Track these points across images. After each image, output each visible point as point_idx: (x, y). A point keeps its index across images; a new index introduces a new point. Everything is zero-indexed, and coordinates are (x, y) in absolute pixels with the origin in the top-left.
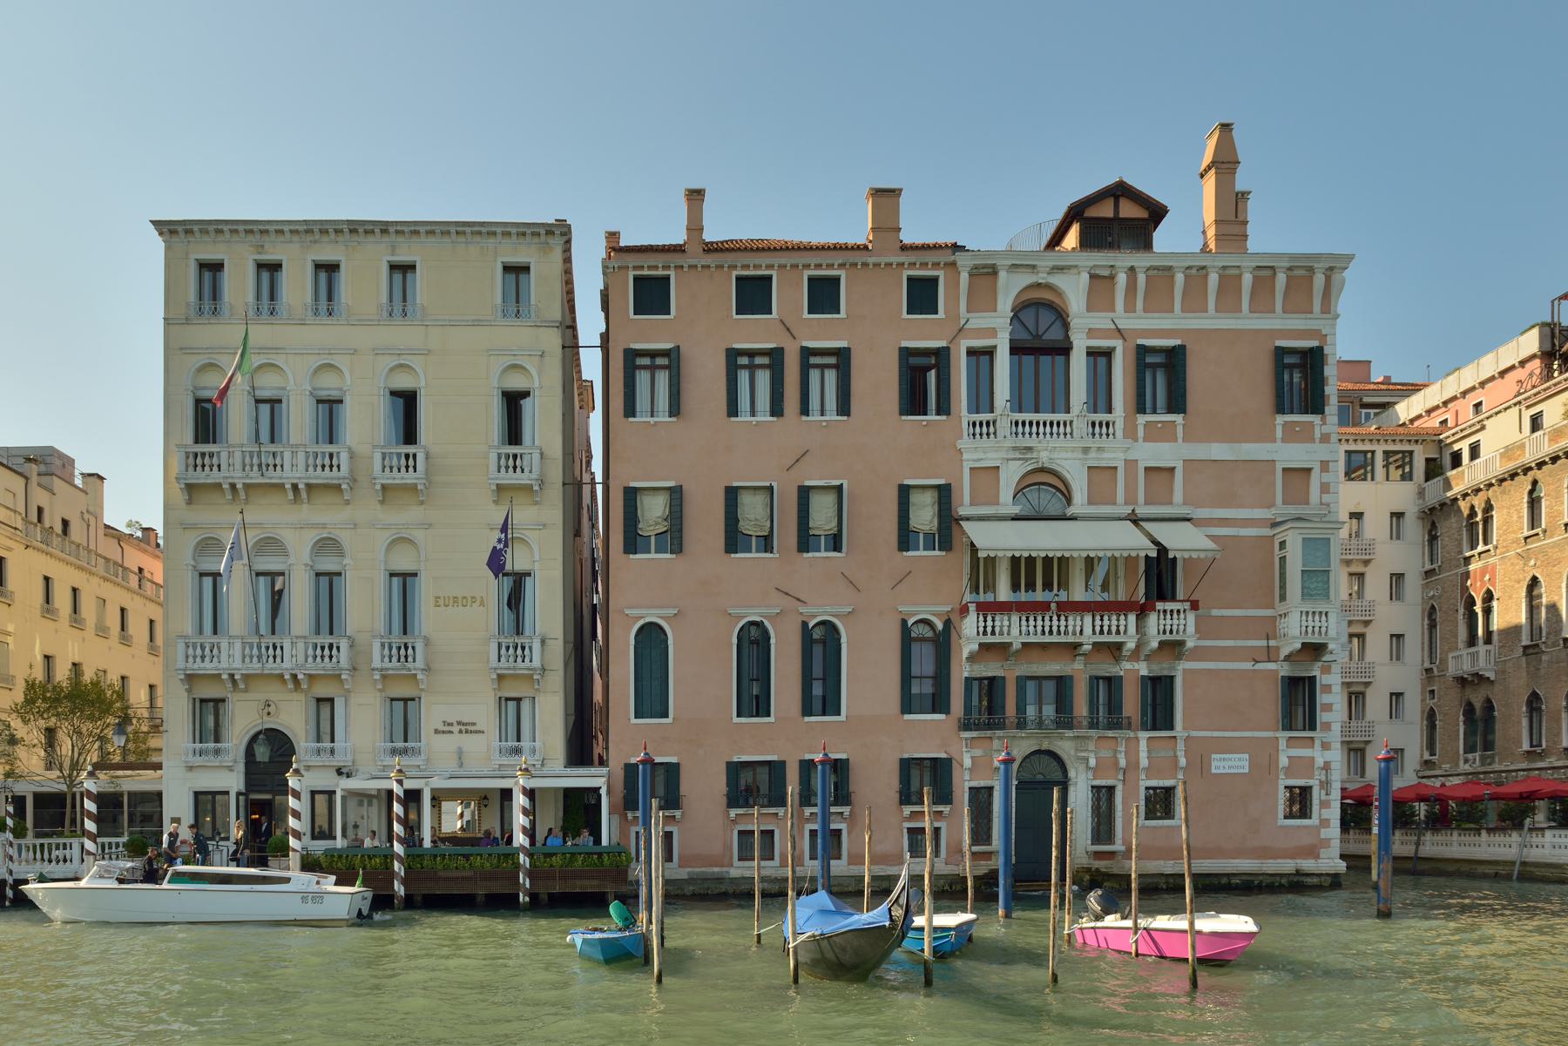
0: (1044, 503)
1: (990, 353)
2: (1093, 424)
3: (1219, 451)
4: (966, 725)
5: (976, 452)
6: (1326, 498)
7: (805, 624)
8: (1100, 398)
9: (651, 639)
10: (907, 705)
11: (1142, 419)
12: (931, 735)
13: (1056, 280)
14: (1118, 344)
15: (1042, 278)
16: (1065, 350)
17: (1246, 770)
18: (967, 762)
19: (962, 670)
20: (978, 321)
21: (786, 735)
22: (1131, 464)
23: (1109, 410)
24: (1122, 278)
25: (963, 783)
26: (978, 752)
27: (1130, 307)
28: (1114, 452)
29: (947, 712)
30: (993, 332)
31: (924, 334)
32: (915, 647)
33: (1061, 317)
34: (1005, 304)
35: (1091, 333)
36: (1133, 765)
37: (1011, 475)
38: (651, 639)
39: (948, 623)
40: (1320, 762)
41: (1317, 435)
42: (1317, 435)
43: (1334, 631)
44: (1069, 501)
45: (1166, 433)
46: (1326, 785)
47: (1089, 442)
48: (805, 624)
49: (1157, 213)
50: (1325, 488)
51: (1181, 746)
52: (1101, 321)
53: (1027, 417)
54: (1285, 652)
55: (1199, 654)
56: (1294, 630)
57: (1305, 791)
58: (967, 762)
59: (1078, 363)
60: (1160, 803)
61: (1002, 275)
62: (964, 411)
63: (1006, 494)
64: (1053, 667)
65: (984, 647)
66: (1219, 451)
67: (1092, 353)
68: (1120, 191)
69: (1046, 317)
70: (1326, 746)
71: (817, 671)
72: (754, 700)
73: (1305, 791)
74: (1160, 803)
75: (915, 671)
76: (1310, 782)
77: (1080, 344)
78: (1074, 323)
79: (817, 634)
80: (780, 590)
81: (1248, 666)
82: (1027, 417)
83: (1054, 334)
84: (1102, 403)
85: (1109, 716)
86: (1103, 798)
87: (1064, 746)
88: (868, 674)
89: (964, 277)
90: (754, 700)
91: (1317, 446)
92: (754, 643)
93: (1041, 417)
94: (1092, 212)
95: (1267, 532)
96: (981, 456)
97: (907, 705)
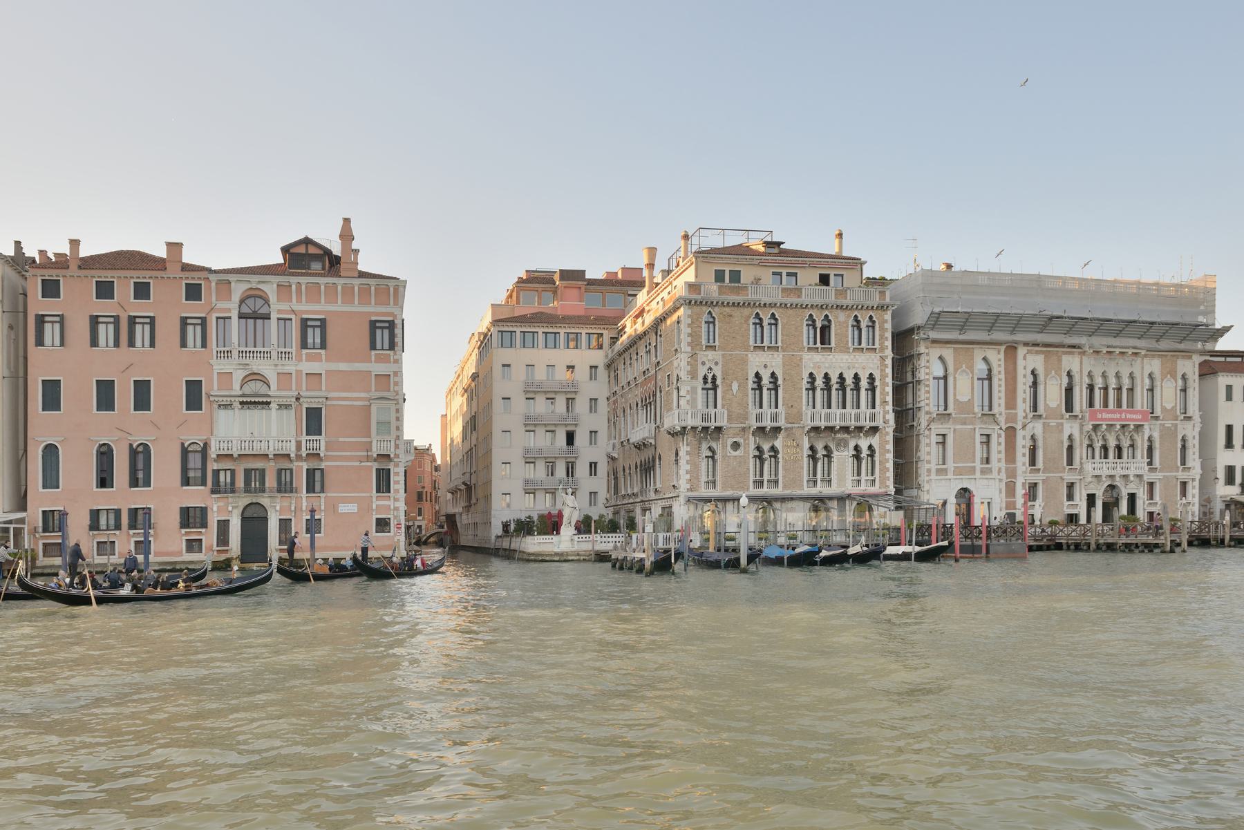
3: (343, 366)
4: (213, 492)
5: (220, 366)
7: (131, 445)
8: (284, 340)
9: (51, 452)
10: (186, 481)
11: (304, 351)
12: (196, 496)
14: (293, 317)
15: (254, 286)
16: (267, 317)
18: (215, 509)
19: (212, 466)
20: (221, 305)
21: (122, 496)
22: (299, 372)
25: (213, 519)
26: (221, 504)
27: (299, 300)
28: (290, 367)
30: (229, 310)
31: (194, 310)
32: (191, 456)
33: (267, 302)
34: (236, 297)
35: (279, 311)
36: (298, 510)
37: (238, 376)
38: (51, 452)
39: (205, 444)
45: (318, 358)
47: (276, 362)
48: (131, 445)
51: (323, 500)
52: (284, 306)
55: (328, 458)
58: (215, 509)
60: (313, 526)
63: (236, 386)
64: (259, 465)
65: (218, 456)
66: (343, 366)
69: (260, 302)
71: (140, 465)
72: (104, 481)
74: (313, 526)
75: (191, 465)
77: (274, 316)
79: (140, 449)
80: (123, 427)
81: (357, 464)
83: (264, 311)
85: (285, 487)
86: (285, 524)
87: (264, 500)
88: (165, 467)
89: (213, 284)
90: (104, 481)
92: (105, 455)
95: (367, 403)
97: (186, 481)
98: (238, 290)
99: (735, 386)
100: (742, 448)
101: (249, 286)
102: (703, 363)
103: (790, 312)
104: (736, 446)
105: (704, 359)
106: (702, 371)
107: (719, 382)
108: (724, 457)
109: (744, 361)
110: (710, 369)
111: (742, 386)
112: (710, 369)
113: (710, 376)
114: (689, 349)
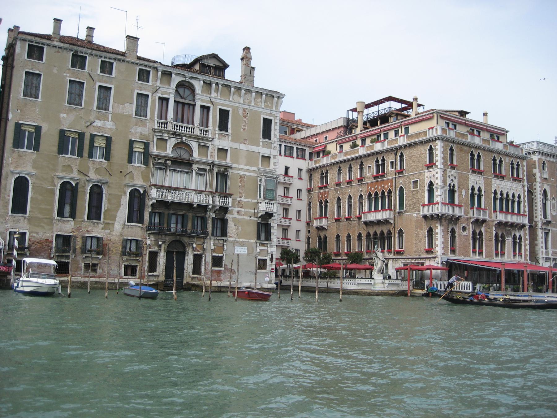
0: (182, 154)
1: (167, 100)
2: (201, 130)
6: (275, 167)
13: (192, 81)
15: (187, 80)
17: (246, 253)
23: (207, 127)
24: (214, 85)
29: (142, 223)
34: (174, 85)
35: (202, 100)
39: (145, 191)
40: (270, 251)
41: (273, 147)
42: (273, 147)
43: (276, 209)
44: (192, 156)
46: (271, 260)
49: (226, 66)
50: (274, 163)
52: (206, 97)
53: (179, 124)
54: (260, 214)
56: (263, 207)
57: (265, 261)
59: (198, 110)
61: (173, 75)
62: (156, 118)
67: (202, 106)
68: (214, 56)
70: (272, 246)
73: (265, 261)
76: (266, 258)
77: (198, 104)
78: (197, 96)
82: (179, 124)
84: (205, 124)
89: (160, 73)
91: (272, 150)
93: (183, 125)
94: (206, 62)
96: (161, 134)
98: (176, 80)
99: (464, 192)
100: (467, 231)
101: (184, 79)
102: (449, 177)
103: (486, 153)
104: (464, 229)
105: (450, 174)
106: (448, 182)
107: (456, 188)
108: (459, 235)
109: (467, 179)
110: (452, 180)
111: (467, 193)
112: (452, 180)
113: (452, 184)
114: (442, 167)
